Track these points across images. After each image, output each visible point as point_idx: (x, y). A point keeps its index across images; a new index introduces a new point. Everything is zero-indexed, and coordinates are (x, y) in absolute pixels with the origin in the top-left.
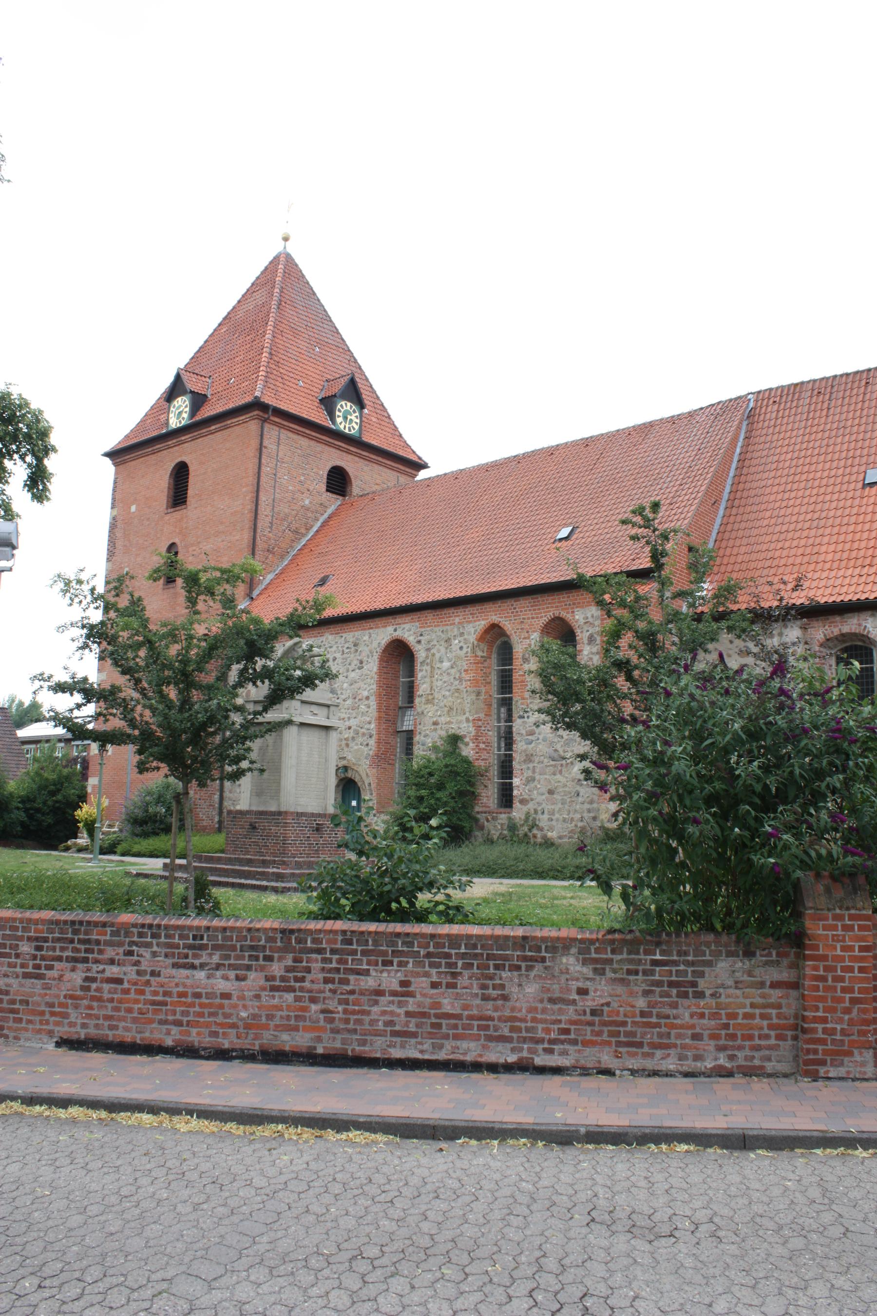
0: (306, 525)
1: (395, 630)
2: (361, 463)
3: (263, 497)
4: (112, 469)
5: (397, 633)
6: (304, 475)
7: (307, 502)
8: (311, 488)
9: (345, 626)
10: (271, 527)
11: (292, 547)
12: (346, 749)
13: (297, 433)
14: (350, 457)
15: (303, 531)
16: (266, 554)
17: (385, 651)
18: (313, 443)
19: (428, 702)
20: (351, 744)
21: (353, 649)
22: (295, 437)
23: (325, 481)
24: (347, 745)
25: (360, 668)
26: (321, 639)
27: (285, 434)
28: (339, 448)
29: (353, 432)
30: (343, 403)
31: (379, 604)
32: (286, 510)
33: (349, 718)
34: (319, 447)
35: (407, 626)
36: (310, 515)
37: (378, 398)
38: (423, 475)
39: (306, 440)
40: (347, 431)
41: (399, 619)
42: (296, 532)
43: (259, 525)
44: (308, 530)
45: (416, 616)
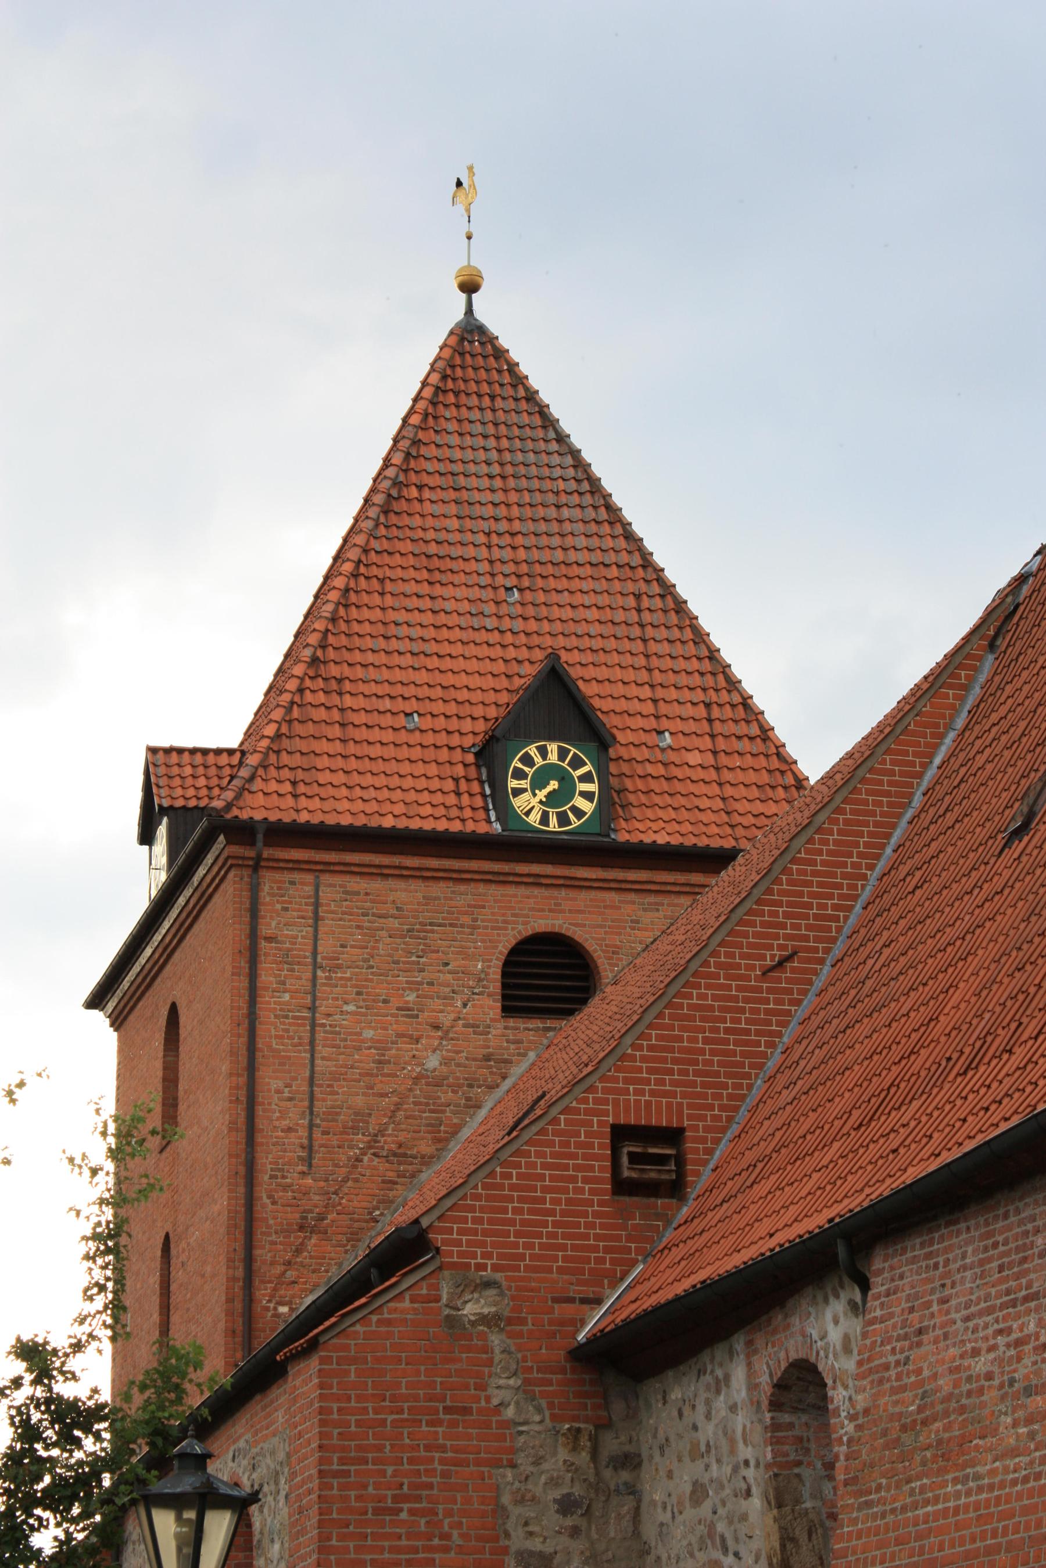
0: (434, 1127)
2: (630, 906)
3: (271, 1081)
4: (111, 1037)
6: (414, 986)
7: (433, 1062)
8: (446, 1019)
10: (309, 1161)
11: (388, 1202)
13: (380, 873)
14: (584, 897)
15: (425, 1147)
16: (299, 1237)
18: (438, 889)
22: (376, 885)
23: (495, 987)
27: (332, 888)
28: (536, 881)
29: (575, 823)
30: (532, 750)
32: (359, 1101)
34: (464, 896)
36: (445, 1096)
37: (733, 684)
39: (413, 885)
40: (553, 825)
43: (265, 1161)
44: (442, 1142)
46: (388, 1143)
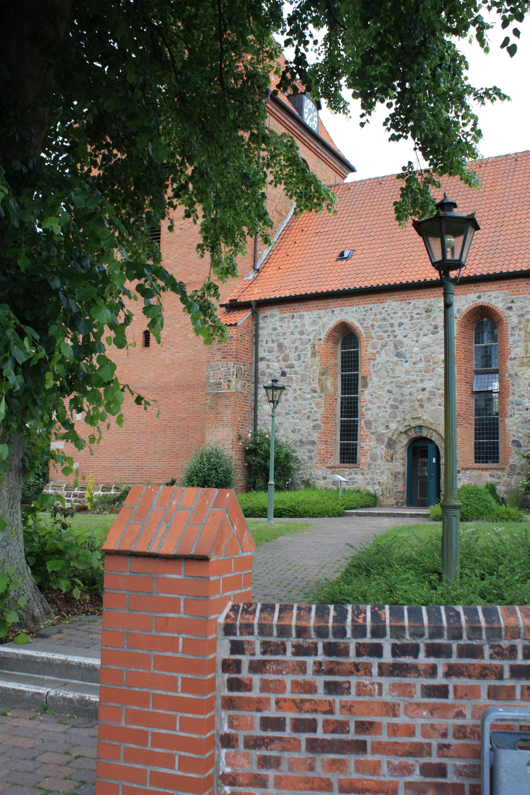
1: (479, 297)
5: (482, 300)
9: (412, 293)
12: (420, 410)
14: (310, 152)
17: (465, 317)
19: (522, 364)
20: (427, 405)
21: (425, 314)
24: (422, 406)
25: (433, 333)
26: (382, 305)
31: (357, 284)
33: (422, 381)
35: (494, 294)
38: (351, 178)
41: (483, 287)
42: (280, 213)
44: (287, 212)
45: (504, 284)
46: (279, 208)
